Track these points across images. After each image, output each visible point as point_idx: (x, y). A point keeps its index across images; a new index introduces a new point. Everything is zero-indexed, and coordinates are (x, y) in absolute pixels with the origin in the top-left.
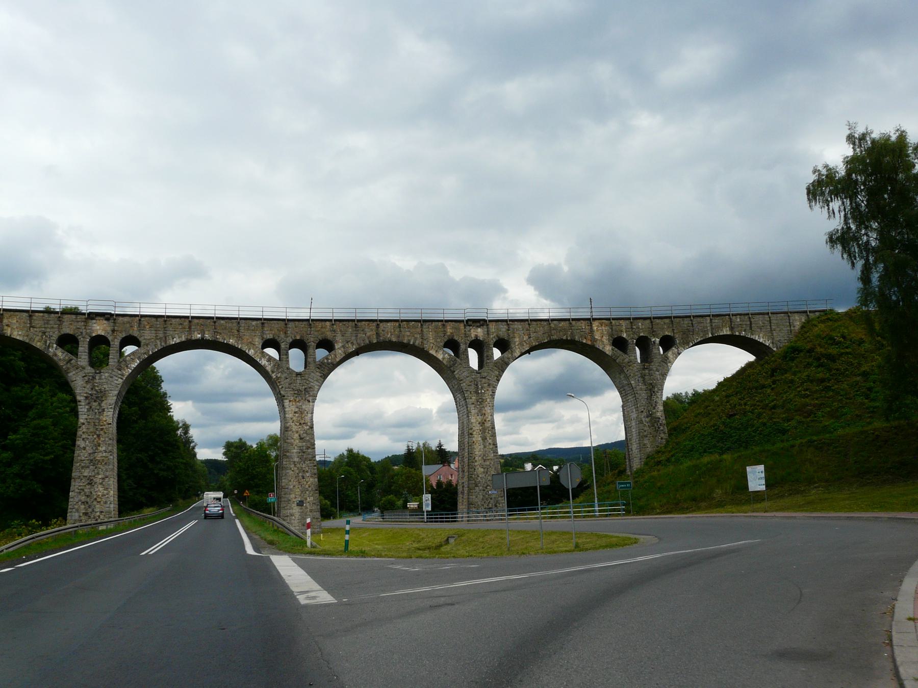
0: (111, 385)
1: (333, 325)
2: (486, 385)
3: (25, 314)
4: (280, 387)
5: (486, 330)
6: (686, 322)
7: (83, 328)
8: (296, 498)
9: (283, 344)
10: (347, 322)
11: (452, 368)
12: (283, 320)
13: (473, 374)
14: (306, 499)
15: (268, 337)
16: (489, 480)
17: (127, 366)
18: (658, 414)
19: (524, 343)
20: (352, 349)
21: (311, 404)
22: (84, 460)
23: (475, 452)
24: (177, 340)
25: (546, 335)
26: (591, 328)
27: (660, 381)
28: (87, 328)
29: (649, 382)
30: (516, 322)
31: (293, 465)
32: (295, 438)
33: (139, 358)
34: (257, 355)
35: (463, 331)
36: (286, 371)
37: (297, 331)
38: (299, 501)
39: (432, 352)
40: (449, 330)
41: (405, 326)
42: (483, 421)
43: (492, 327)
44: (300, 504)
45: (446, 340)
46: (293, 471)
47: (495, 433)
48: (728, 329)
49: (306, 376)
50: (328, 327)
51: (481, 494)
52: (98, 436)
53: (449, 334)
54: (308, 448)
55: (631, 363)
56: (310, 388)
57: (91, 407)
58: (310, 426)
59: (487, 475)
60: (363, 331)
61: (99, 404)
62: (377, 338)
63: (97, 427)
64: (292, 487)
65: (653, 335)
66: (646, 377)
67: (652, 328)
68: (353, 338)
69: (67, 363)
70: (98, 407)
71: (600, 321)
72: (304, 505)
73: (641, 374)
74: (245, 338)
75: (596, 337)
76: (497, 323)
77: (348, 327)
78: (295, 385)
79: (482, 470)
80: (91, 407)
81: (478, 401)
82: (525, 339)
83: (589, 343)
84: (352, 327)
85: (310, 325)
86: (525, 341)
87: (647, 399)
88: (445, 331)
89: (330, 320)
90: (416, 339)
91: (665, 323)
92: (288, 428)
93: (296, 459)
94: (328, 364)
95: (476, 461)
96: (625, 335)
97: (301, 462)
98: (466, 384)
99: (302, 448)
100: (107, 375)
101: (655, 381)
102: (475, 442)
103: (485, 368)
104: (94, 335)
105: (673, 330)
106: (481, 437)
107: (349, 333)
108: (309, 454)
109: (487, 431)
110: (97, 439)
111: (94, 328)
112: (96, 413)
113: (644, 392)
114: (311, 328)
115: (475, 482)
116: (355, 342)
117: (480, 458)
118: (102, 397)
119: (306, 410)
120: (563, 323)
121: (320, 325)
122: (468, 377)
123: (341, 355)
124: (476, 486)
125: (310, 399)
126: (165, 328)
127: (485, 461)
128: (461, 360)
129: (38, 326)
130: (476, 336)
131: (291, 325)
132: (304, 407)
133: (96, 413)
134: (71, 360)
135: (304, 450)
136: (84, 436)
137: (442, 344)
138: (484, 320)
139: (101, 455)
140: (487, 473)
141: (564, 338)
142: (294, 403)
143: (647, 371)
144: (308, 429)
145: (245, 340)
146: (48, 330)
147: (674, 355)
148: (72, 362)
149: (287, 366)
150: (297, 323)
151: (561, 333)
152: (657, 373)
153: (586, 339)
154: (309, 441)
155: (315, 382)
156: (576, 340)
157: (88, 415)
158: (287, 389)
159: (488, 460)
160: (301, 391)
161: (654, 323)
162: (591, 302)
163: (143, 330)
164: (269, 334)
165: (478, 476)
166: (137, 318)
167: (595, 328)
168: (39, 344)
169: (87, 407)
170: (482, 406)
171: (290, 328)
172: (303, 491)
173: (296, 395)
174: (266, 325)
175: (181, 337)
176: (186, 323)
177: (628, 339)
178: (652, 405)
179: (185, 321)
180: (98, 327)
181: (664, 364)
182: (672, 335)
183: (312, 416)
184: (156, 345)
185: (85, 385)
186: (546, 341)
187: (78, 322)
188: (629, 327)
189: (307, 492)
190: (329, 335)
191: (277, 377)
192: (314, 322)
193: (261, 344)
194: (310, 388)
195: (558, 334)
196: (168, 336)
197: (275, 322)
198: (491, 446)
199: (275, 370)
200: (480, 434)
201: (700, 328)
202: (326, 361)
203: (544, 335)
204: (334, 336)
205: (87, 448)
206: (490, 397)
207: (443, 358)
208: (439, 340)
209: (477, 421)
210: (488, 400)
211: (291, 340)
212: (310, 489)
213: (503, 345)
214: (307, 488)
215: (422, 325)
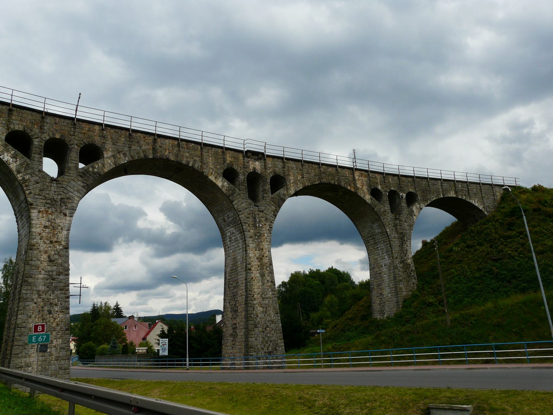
1: (103, 130)
2: (263, 219)
4: (27, 192)
5: (263, 164)
6: (424, 183)
9: (36, 140)
15: (17, 128)
16: (268, 321)
18: (409, 261)
19: (298, 182)
21: (68, 218)
23: (254, 289)
25: (318, 177)
26: (354, 177)
27: (408, 231)
29: (400, 231)
30: (290, 161)
31: (36, 296)
32: (42, 259)
35: (242, 162)
36: (37, 173)
37: (57, 128)
40: (228, 158)
41: (185, 146)
43: (269, 161)
46: (35, 303)
48: (454, 192)
50: (97, 131)
51: (260, 336)
53: (228, 162)
54: (59, 274)
55: (386, 213)
56: (68, 198)
58: (64, 246)
59: (266, 315)
62: (153, 154)
65: (401, 190)
66: (398, 227)
67: (400, 184)
68: (126, 149)
71: (360, 172)
72: (48, 350)
73: (394, 223)
75: (358, 186)
76: (274, 160)
78: (48, 192)
79: (261, 309)
83: (353, 190)
84: (125, 137)
86: (299, 180)
87: (399, 246)
88: (224, 158)
90: (195, 161)
91: (409, 181)
92: (33, 245)
93: (42, 288)
94: (94, 173)
95: (255, 299)
96: (380, 188)
97: (48, 291)
98: (245, 216)
99: (51, 273)
101: (404, 231)
102: (254, 278)
105: (415, 188)
106: (259, 273)
107: (122, 142)
108: (60, 282)
109: (265, 267)
113: (397, 240)
114: (75, 128)
115: (255, 322)
116: (128, 153)
117: (259, 296)
119: (60, 226)
120: (330, 169)
121: (86, 127)
123: (110, 165)
124: (256, 327)
125: (67, 212)
127: (264, 299)
128: (240, 190)
130: (254, 169)
131: (49, 120)
132: (58, 221)
138: (263, 154)
140: (266, 312)
141: (333, 182)
142: (44, 215)
143: (398, 222)
144: (61, 249)
147: (418, 210)
149: (40, 168)
150: (57, 119)
151: (330, 178)
152: (406, 224)
153: (350, 186)
155: (76, 193)
158: (36, 196)
159: (267, 298)
160: (55, 201)
161: (400, 180)
165: (257, 316)
167: (357, 177)
170: (260, 241)
171: (47, 123)
173: (48, 205)
177: (382, 191)
178: (403, 252)
181: (410, 216)
182: (415, 192)
183: (68, 234)
186: (317, 183)
188: (383, 181)
189: (54, 333)
190: (97, 141)
191: (24, 179)
192: (80, 123)
193: (5, 134)
197: (27, 112)
199: (23, 170)
201: (434, 189)
203: (316, 177)
204: (103, 143)
206: (268, 232)
207: (223, 186)
210: (266, 235)
211: (48, 138)
214: (54, 328)
215: (201, 148)
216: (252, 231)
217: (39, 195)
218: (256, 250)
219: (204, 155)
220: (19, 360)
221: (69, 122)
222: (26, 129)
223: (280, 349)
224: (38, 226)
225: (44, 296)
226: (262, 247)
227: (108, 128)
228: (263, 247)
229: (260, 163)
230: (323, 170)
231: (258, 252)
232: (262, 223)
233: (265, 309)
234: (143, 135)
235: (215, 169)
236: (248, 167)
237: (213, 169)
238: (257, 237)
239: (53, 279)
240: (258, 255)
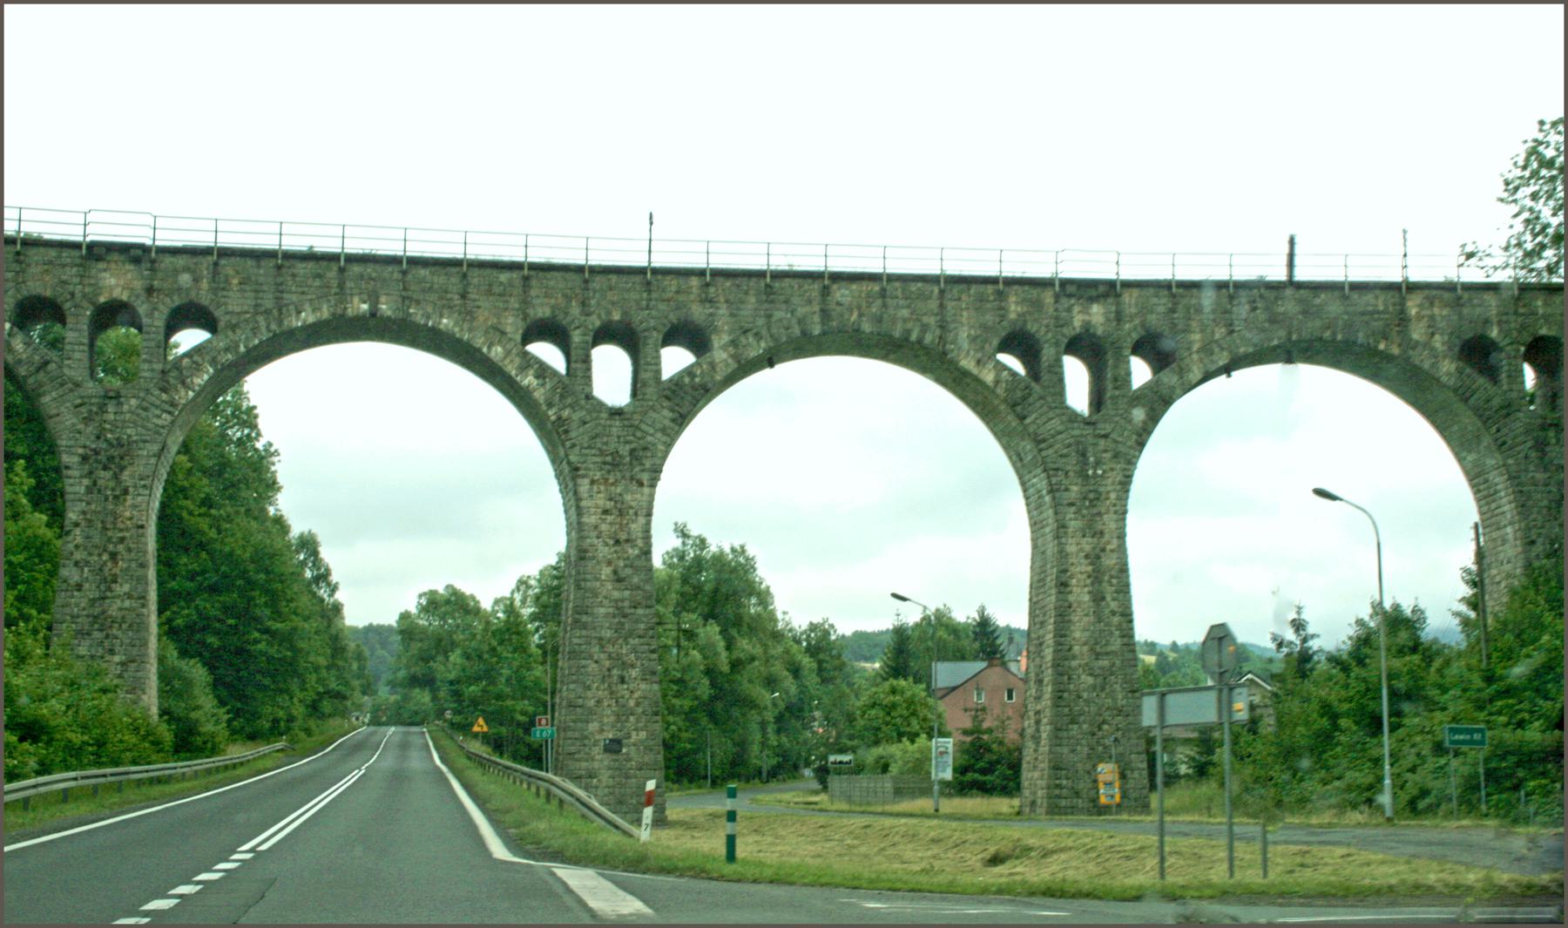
0: (143, 427)
1: (707, 285)
2: (1108, 455)
7: (76, 280)
9: (577, 332)
10: (745, 279)
11: (1018, 408)
12: (579, 269)
13: (1076, 425)
16: (1108, 708)
17: (183, 383)
19: (1214, 345)
20: (756, 350)
21: (646, 490)
22: (78, 617)
24: (308, 317)
28: (86, 281)
31: (597, 649)
33: (213, 362)
34: (512, 361)
35: (1051, 310)
38: (611, 740)
39: (968, 363)
40: (1013, 307)
41: (899, 293)
43: (1129, 299)
44: (614, 747)
46: (596, 662)
47: (1127, 585)
52: (114, 556)
53: (1013, 316)
56: (645, 449)
58: (641, 549)
60: (786, 302)
61: (116, 477)
62: (823, 323)
64: (592, 703)
68: (761, 322)
69: (38, 370)
70: (112, 484)
71: (1426, 292)
72: (624, 750)
74: (482, 315)
77: (746, 293)
78: (605, 439)
79: (1090, 680)
80: (95, 483)
81: (1085, 498)
82: (1217, 336)
83: (1395, 351)
85: (649, 283)
86: (1216, 341)
87: (1549, 509)
88: (1001, 308)
90: (925, 328)
92: (586, 551)
93: (608, 634)
94: (694, 388)
95: (1074, 657)
99: (620, 604)
100: (133, 402)
102: (1075, 605)
104: (102, 300)
106: (1089, 592)
108: (637, 621)
110: (109, 564)
112: (106, 499)
114: (649, 292)
116: (764, 332)
117: (1085, 648)
118: (122, 458)
119: (631, 507)
121: (672, 284)
122: (1061, 433)
123: (727, 365)
124: (1073, 722)
125: (645, 477)
126: (281, 284)
127: (1098, 656)
128: (1044, 387)
130: (1087, 326)
131: (598, 282)
132: (628, 497)
133: (106, 499)
134: (46, 363)
136: (78, 556)
137: (995, 342)
140: (1103, 689)
141: (1327, 334)
142: (602, 488)
145: (481, 319)
148: (52, 366)
149: (587, 390)
150: (614, 278)
154: (638, 588)
155: (659, 435)
157: (88, 503)
158: (587, 451)
159: (1107, 653)
163: (223, 289)
165: (1079, 697)
166: (210, 258)
167: (1413, 312)
169: (86, 482)
170: (1095, 511)
172: (622, 714)
173: (608, 467)
174: (534, 282)
175: (320, 309)
176: (332, 274)
179: (329, 269)
180: (113, 281)
183: (648, 523)
184: (255, 331)
185: (81, 427)
187: (64, 266)
189: (632, 718)
190: (698, 313)
191: (559, 418)
192: (660, 277)
193: (521, 331)
194: (645, 449)
196: (287, 305)
197: (555, 274)
198: (1116, 619)
202: (687, 380)
204: (711, 315)
205: (87, 586)
206: (1119, 487)
207: (997, 382)
209: (1081, 550)
210: (1113, 496)
211: (598, 323)
212: (640, 710)
215: (942, 292)
216: (1075, 488)
217: (589, 447)
218: (1084, 536)
219: (949, 308)
221: (638, 279)
222: (557, 312)
223: (1136, 774)
224: (593, 510)
225: (610, 649)
226: (1099, 527)
231: (1090, 540)
234: (797, 280)
240: (1087, 548)
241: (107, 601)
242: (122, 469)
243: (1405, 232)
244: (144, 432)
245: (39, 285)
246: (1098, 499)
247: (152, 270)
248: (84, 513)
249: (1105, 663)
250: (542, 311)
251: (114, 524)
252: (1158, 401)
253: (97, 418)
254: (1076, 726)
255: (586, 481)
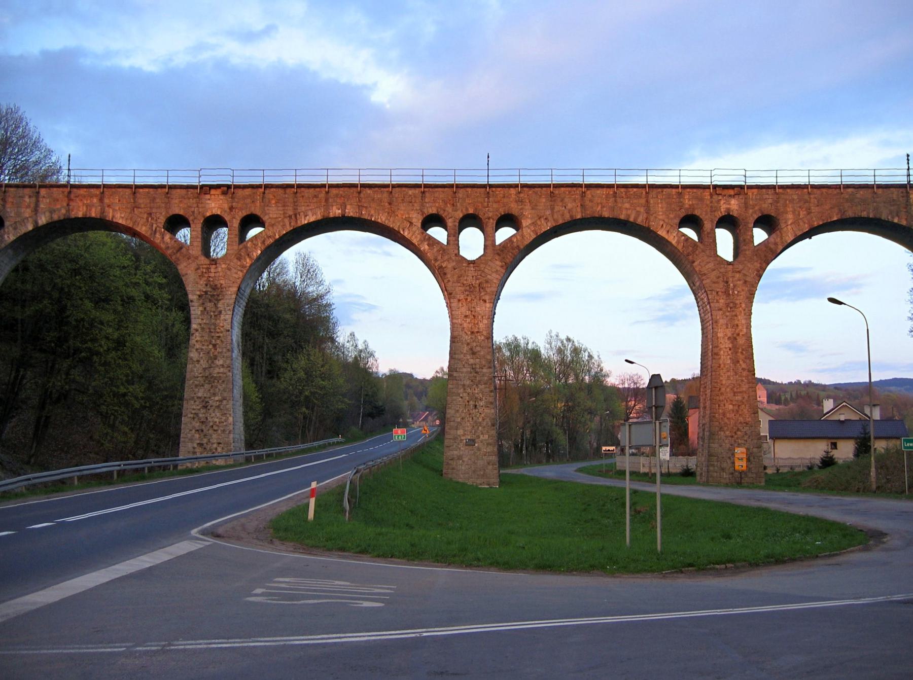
2: (741, 283)
3: (128, 191)
8: (464, 435)
9: (450, 220)
10: (540, 189)
11: (690, 257)
12: (451, 186)
13: (722, 266)
14: (478, 437)
16: (741, 423)
20: (546, 227)
22: (198, 377)
25: (836, 210)
28: (200, 205)
30: (788, 190)
31: (462, 390)
38: (469, 440)
39: (662, 233)
42: (735, 335)
44: (471, 443)
45: (682, 215)
46: (462, 397)
49: (482, 266)
52: (215, 346)
53: (687, 206)
57: (205, 308)
62: (582, 213)
63: (213, 334)
68: (548, 212)
70: (213, 309)
74: (399, 213)
77: (540, 196)
79: (731, 407)
80: (205, 308)
81: (727, 306)
86: (801, 219)
89: (516, 186)
90: (638, 213)
93: (468, 382)
98: (711, 281)
99: (474, 366)
100: (223, 266)
102: (722, 366)
103: (741, 258)
104: (208, 214)
106: (730, 359)
107: (542, 204)
108: (483, 375)
110: (213, 350)
111: (207, 206)
116: (550, 218)
118: (218, 296)
119: (480, 314)
120: (862, 192)
124: (721, 429)
125: (487, 298)
129: (142, 206)
130: (728, 210)
135: (478, 370)
136: (197, 346)
137: (677, 221)
139: (217, 370)
140: (738, 411)
141: (864, 214)
144: (483, 340)
146: (154, 210)
150: (469, 190)
156: (883, 218)
159: (740, 392)
160: (474, 287)
162: (908, 160)
164: (431, 207)
168: (144, 228)
169: (201, 308)
170: (734, 314)
173: (467, 293)
174: (427, 195)
176: (322, 195)
179: (321, 192)
180: (213, 205)
184: (284, 226)
190: (514, 209)
192: (494, 189)
193: (421, 221)
194: (487, 282)
195: (854, 208)
199: (439, 258)
200: (729, 355)
204: (522, 209)
208: (672, 216)
210: (743, 305)
211: (461, 216)
213: (767, 222)
214: (480, 423)
218: (727, 328)
219: (652, 202)
220: (452, 453)
226: (736, 322)
227: (525, 189)
228: (738, 322)
229: (738, 201)
230: (847, 197)
232: (739, 289)
233: (736, 408)
235: (666, 220)
236: (718, 209)
237: (664, 221)
238: (729, 309)
239: (477, 373)
240: (729, 335)
241: (212, 369)
242: (218, 300)
243: (908, 156)
244: (229, 282)
245: (177, 209)
246: (735, 307)
247: (232, 198)
248: (200, 324)
249: (739, 398)
250: (432, 210)
251: (215, 329)
252: (770, 253)
253: (206, 275)
254: (722, 433)
255: (456, 300)
